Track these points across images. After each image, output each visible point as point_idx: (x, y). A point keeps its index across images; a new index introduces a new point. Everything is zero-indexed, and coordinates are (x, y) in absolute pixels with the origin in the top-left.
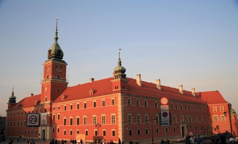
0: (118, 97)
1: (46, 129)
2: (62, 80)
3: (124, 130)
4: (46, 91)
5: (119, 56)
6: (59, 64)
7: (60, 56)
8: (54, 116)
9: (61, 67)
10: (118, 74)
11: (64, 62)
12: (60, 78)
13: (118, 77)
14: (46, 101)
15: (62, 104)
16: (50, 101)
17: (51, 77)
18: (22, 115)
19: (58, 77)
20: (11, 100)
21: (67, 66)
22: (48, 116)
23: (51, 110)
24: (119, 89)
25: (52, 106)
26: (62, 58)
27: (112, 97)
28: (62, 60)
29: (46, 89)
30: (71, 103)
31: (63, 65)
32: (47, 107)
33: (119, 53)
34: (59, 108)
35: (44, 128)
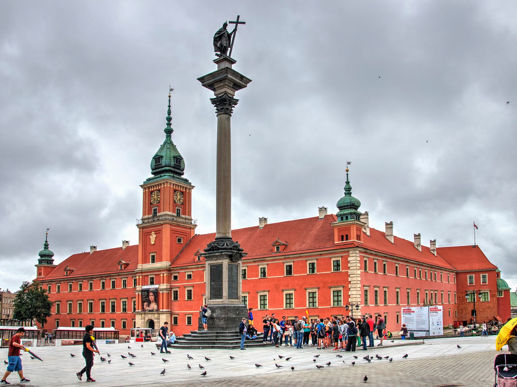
4: (153, 243)
6: (179, 186)
9: (182, 193)
14: (153, 261)
15: (198, 268)
18: (81, 289)
19: (177, 213)
20: (44, 258)
21: (193, 191)
22: (161, 292)
26: (183, 174)
29: (153, 238)
31: (186, 188)
34: (190, 276)
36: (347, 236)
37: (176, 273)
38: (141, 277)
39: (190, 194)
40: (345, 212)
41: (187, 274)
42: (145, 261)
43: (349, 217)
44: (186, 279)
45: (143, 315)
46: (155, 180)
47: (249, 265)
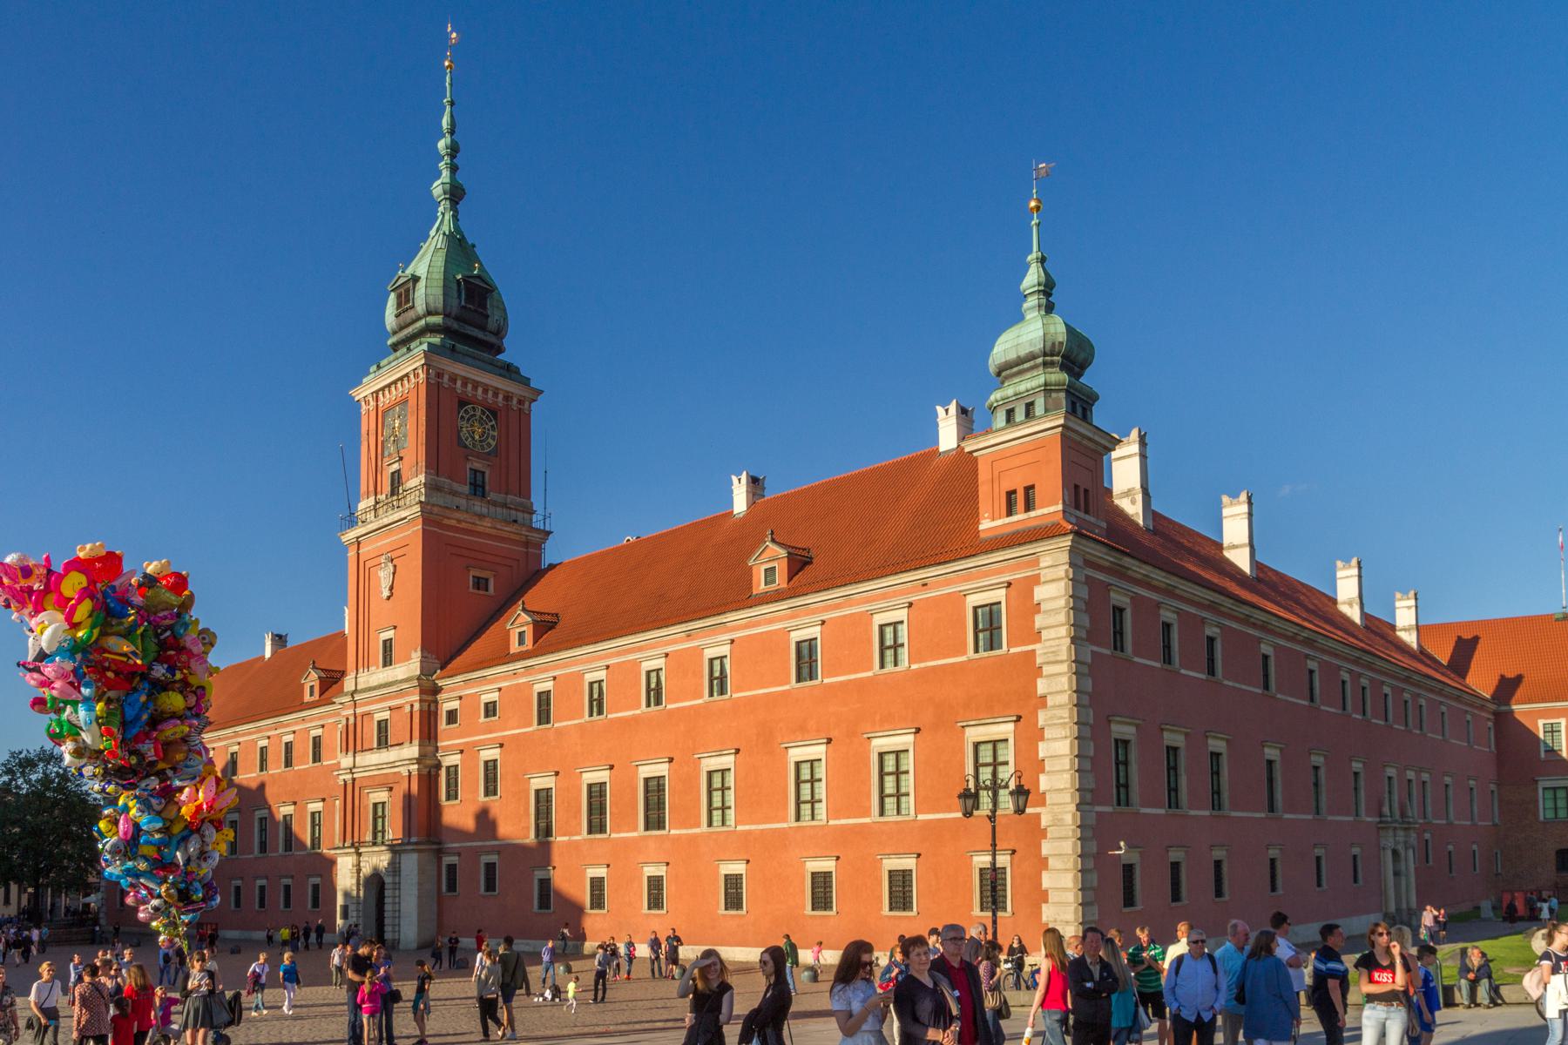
2: (505, 505)
3: (1090, 864)
4: (386, 593)
8: (452, 771)
9: (494, 413)
10: (1041, 380)
11: (509, 371)
12: (492, 496)
14: (387, 662)
16: (416, 656)
17: (422, 478)
19: (474, 485)
22: (404, 771)
23: (429, 734)
24: (1050, 509)
25: (440, 697)
26: (500, 350)
27: (978, 585)
29: (384, 576)
30: (590, 663)
31: (508, 398)
32: (399, 708)
34: (490, 709)
36: (1029, 489)
37: (450, 700)
38: (352, 721)
40: (1022, 387)
41: (486, 698)
42: (363, 663)
43: (1039, 409)
44: (482, 719)
47: (669, 649)
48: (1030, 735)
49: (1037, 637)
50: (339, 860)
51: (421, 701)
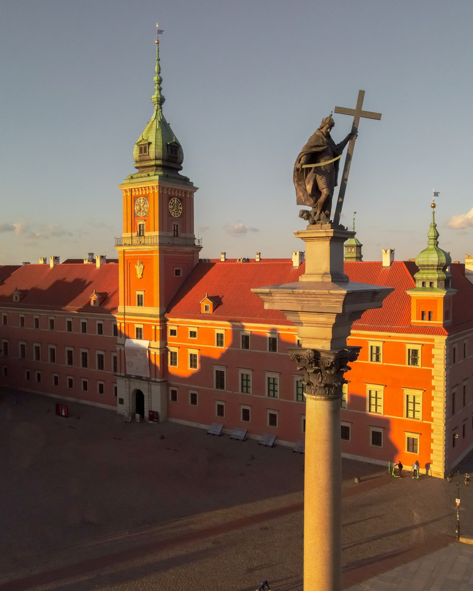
0: (433, 346)
1: (150, 391)
4: (139, 276)
5: (432, 215)
7: (175, 162)
8: (174, 354)
11: (186, 180)
13: (435, 285)
14: (140, 304)
22: (152, 353)
26: (181, 169)
28: (180, 172)
29: (139, 269)
31: (186, 192)
33: (434, 207)
34: (193, 334)
35: (137, 385)
38: (123, 325)
39: (191, 200)
41: (191, 329)
42: (128, 302)
45: (127, 382)
46: (141, 180)
48: (428, 399)
49: (433, 366)
50: (118, 380)
51: (160, 325)
